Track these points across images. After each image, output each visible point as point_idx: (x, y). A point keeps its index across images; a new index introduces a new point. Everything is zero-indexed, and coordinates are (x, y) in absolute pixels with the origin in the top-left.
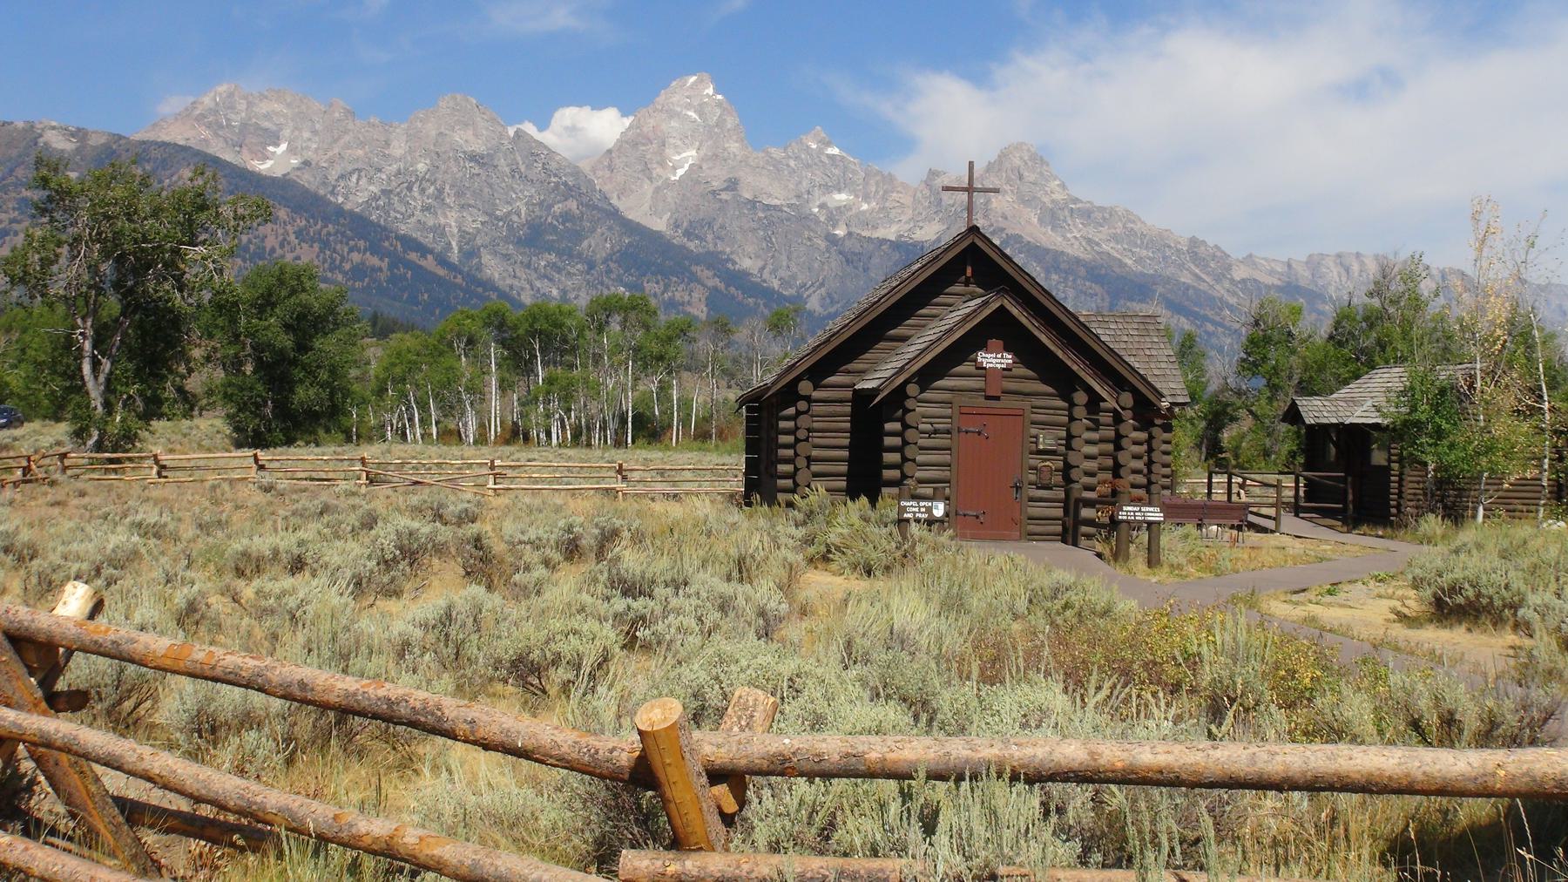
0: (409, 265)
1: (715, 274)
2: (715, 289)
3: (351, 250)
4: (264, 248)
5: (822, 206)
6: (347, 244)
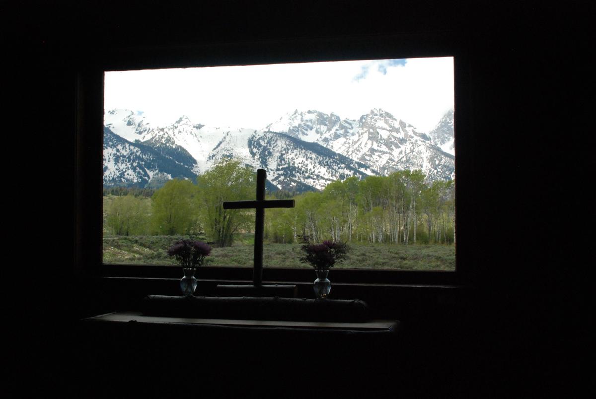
0: (361, 173)
3: (339, 168)
4: (307, 169)
6: (337, 166)
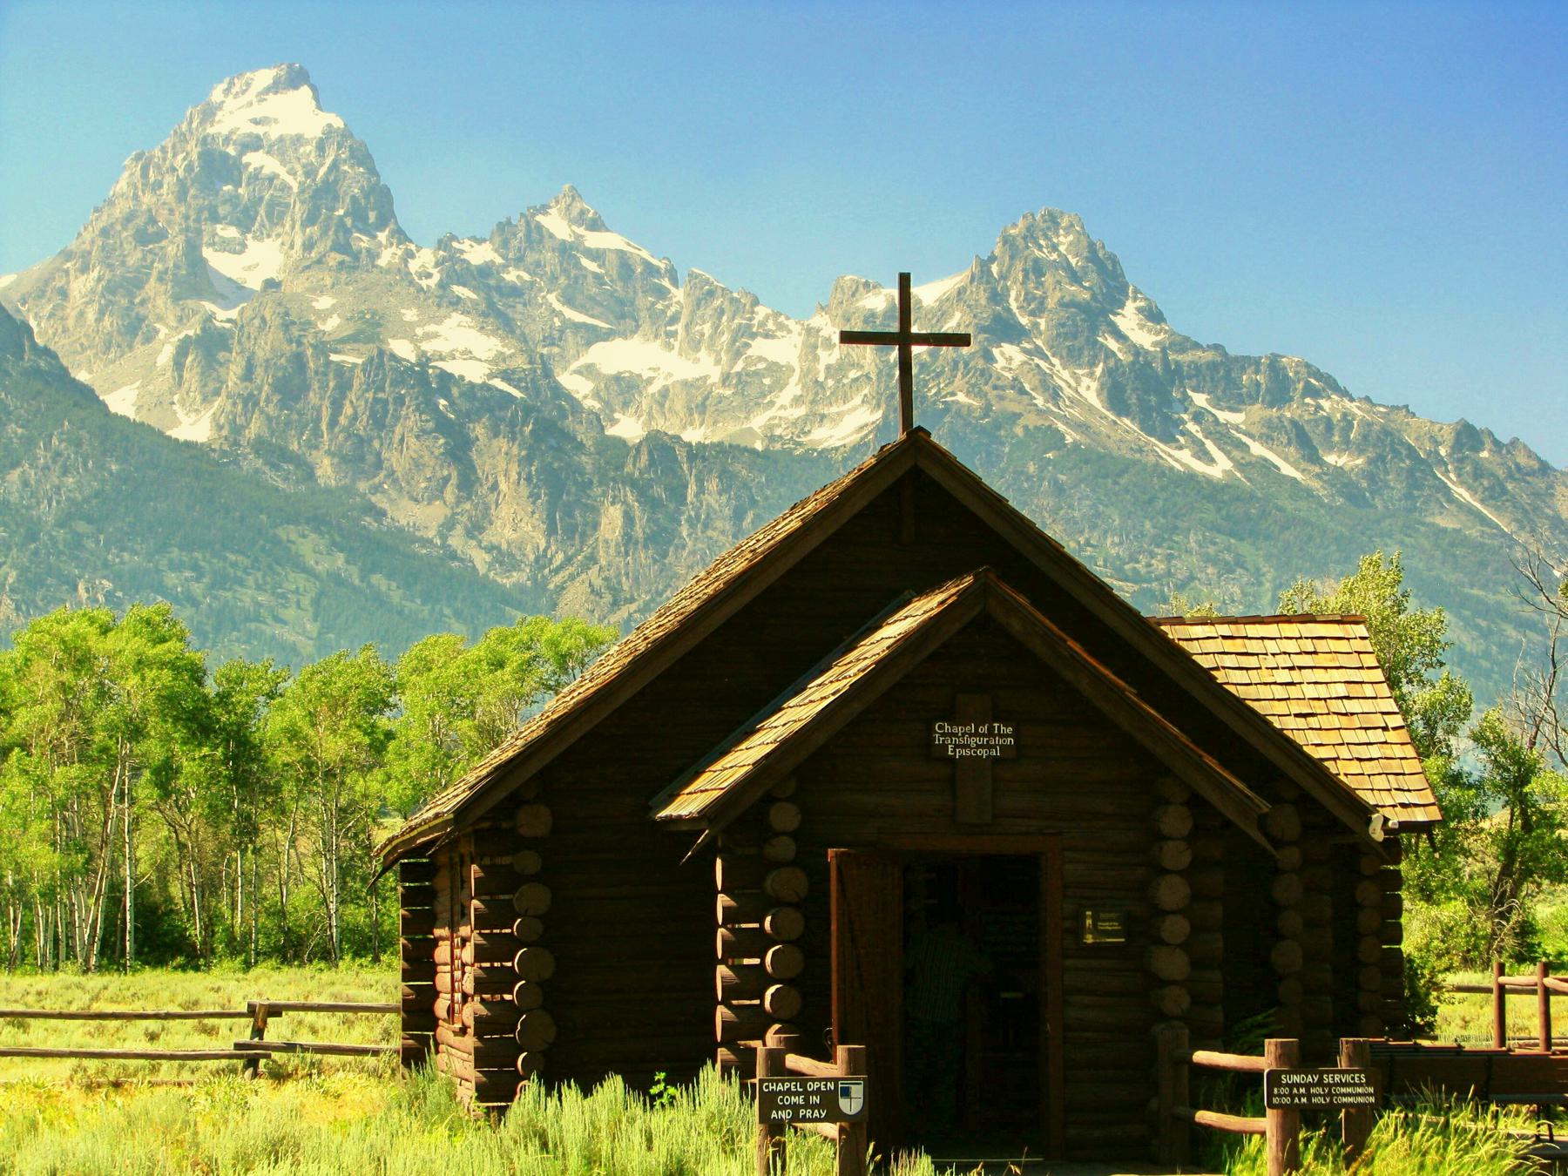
1: (334, 544)
2: (337, 579)
5: (588, 371)
